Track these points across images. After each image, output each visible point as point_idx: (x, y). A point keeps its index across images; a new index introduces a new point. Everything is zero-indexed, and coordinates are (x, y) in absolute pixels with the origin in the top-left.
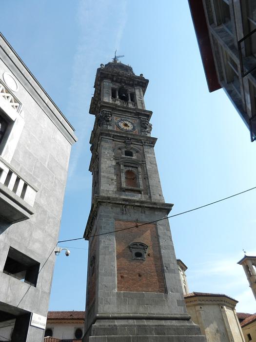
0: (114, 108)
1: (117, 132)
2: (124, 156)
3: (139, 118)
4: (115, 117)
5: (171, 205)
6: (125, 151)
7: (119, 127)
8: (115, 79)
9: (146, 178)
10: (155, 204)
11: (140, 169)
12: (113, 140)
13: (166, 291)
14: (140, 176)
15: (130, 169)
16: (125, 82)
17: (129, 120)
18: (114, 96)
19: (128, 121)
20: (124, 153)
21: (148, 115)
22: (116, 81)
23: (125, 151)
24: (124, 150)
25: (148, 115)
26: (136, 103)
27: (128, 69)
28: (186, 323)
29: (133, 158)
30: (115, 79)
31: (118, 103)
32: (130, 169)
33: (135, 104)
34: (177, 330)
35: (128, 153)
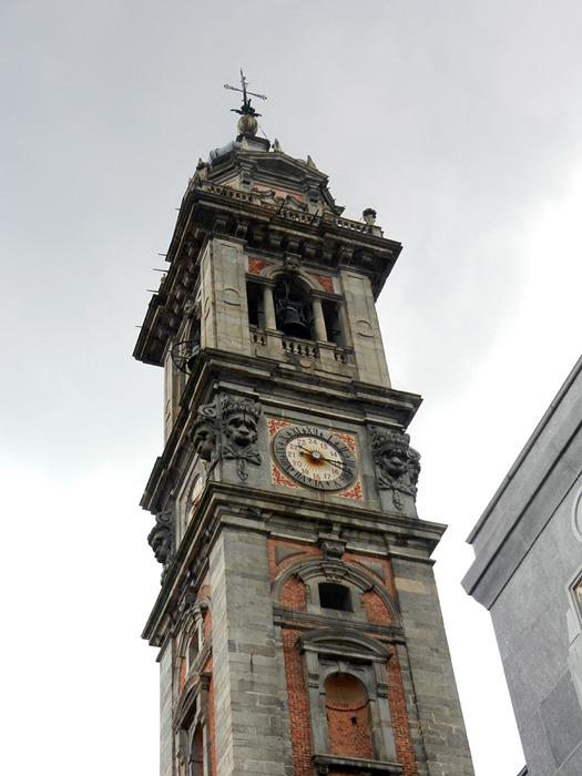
2: (315, 609)
3: (365, 424)
4: (268, 420)
6: (321, 586)
7: (284, 465)
12: (267, 534)
15: (343, 668)
16: (301, 250)
17: (326, 433)
18: (255, 316)
19: (321, 438)
20: (316, 595)
21: (404, 407)
23: (321, 586)
24: (313, 583)
25: (404, 407)
26: (352, 351)
27: (310, 181)
31: (276, 348)
32: (343, 668)
33: (345, 354)
35: (334, 597)
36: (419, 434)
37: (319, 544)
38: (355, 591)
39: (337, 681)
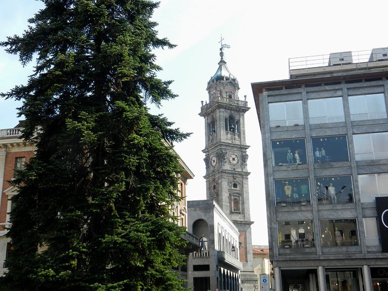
0: (227, 145)
1: (230, 170)
2: (233, 188)
5: (253, 222)
7: (230, 162)
8: (227, 107)
9: (243, 203)
10: (247, 222)
11: (240, 197)
13: (247, 262)
14: (240, 203)
21: (247, 147)
22: (228, 109)
24: (233, 184)
25: (247, 147)
28: (253, 273)
29: (237, 189)
30: (227, 107)
32: (236, 197)
33: (239, 136)
34: (250, 275)
36: (248, 152)
37: (233, 177)
38: (238, 184)
39: (235, 199)
